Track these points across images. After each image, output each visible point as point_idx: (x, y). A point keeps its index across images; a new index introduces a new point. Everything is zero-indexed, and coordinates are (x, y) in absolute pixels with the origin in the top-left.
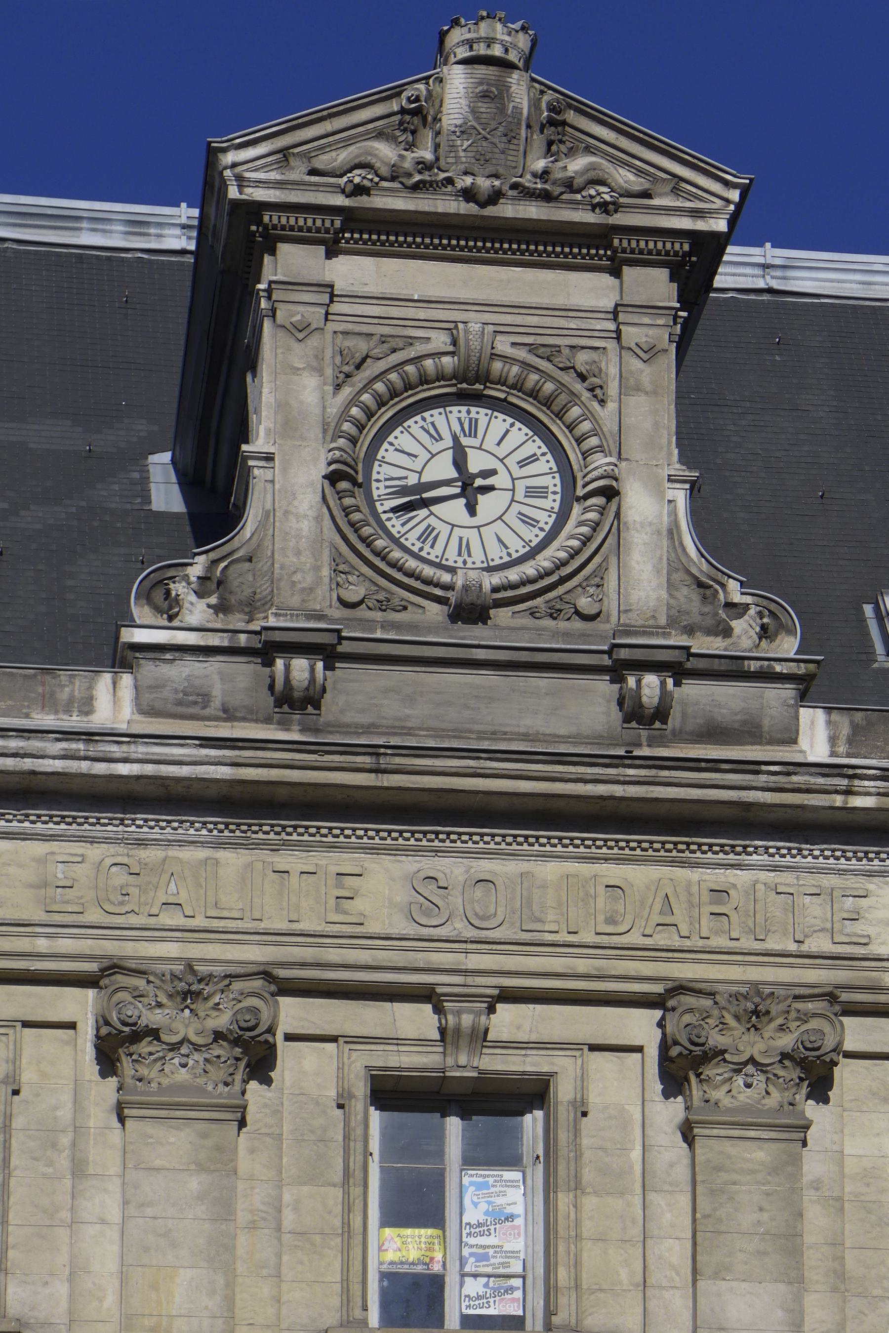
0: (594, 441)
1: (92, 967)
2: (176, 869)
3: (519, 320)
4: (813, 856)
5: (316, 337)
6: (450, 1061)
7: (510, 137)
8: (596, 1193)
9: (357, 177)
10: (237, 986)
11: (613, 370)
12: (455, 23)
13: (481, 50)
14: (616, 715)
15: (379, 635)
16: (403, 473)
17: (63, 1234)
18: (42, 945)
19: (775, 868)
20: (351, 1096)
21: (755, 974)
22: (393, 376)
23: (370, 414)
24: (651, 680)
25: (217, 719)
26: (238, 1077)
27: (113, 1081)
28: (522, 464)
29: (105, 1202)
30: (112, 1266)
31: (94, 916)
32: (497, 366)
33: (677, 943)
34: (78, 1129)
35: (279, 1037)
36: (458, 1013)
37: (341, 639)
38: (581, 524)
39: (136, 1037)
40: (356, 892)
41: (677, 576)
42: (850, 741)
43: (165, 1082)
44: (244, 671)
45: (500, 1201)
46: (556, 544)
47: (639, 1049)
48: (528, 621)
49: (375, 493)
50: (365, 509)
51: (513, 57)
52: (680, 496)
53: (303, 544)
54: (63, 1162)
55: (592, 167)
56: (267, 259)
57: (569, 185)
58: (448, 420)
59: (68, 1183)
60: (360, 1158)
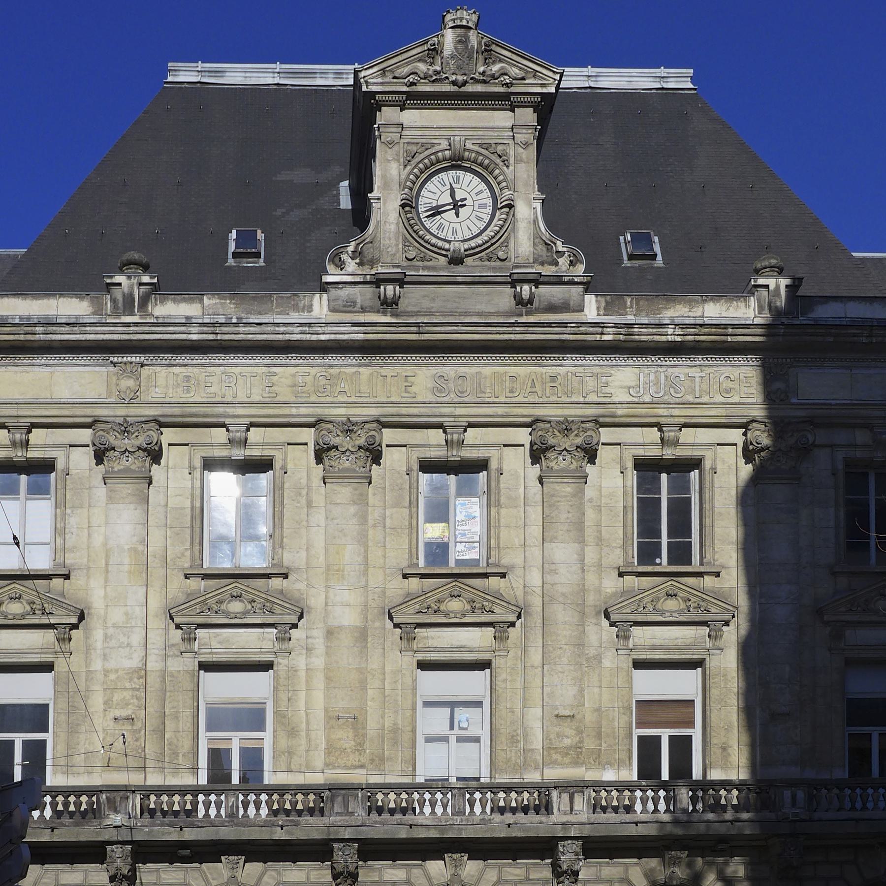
0: (504, 184)
1: (312, 420)
2: (344, 377)
3: (475, 133)
4: (590, 360)
5: (397, 146)
6: (450, 454)
7: (470, 57)
8: (506, 507)
9: (411, 79)
10: (367, 426)
11: (512, 153)
12: (448, 12)
13: (458, 23)
14: (513, 302)
15: (420, 273)
16: (431, 201)
17: (304, 531)
18: (294, 411)
19: (575, 366)
20: (412, 470)
21: (567, 412)
22: (426, 161)
23: (417, 177)
24: (526, 287)
25: (359, 312)
26: (368, 464)
27: (321, 465)
28: (477, 194)
29: (319, 517)
30: (322, 544)
31: (313, 399)
32: (467, 154)
33: (537, 400)
34: (309, 488)
35: (384, 446)
36: (452, 434)
37: (406, 275)
38: (499, 220)
39: (329, 449)
40: (413, 383)
41: (537, 240)
42: (605, 309)
43: (341, 467)
44: (369, 290)
45: (470, 511)
46: (490, 229)
47: (523, 445)
48: (479, 263)
49: (420, 211)
50: (416, 218)
51: (470, 25)
52: (538, 205)
53: (392, 235)
54: (303, 501)
55: (502, 68)
56: (378, 113)
57: (493, 77)
58: (447, 177)
59: (305, 510)
60: (415, 496)
